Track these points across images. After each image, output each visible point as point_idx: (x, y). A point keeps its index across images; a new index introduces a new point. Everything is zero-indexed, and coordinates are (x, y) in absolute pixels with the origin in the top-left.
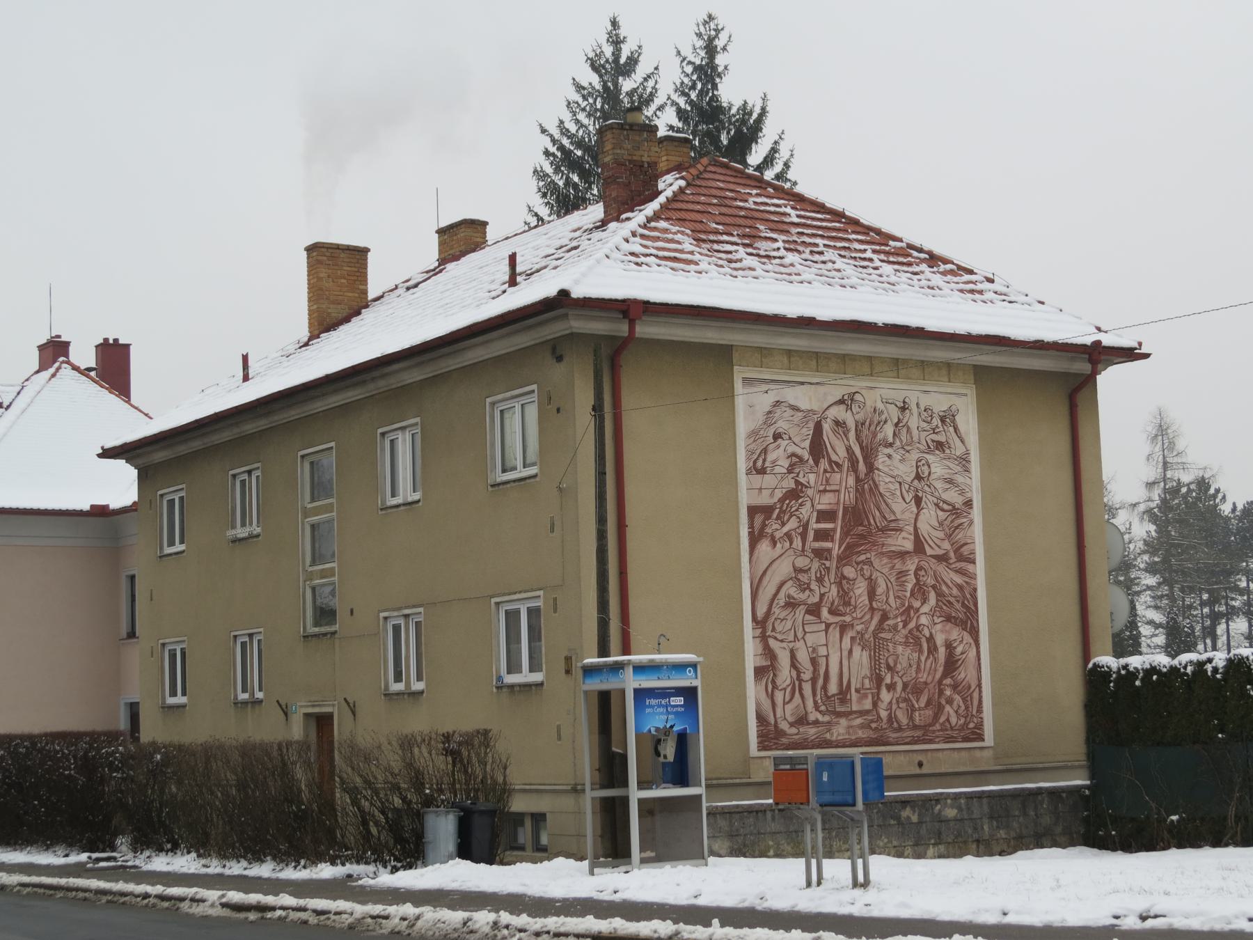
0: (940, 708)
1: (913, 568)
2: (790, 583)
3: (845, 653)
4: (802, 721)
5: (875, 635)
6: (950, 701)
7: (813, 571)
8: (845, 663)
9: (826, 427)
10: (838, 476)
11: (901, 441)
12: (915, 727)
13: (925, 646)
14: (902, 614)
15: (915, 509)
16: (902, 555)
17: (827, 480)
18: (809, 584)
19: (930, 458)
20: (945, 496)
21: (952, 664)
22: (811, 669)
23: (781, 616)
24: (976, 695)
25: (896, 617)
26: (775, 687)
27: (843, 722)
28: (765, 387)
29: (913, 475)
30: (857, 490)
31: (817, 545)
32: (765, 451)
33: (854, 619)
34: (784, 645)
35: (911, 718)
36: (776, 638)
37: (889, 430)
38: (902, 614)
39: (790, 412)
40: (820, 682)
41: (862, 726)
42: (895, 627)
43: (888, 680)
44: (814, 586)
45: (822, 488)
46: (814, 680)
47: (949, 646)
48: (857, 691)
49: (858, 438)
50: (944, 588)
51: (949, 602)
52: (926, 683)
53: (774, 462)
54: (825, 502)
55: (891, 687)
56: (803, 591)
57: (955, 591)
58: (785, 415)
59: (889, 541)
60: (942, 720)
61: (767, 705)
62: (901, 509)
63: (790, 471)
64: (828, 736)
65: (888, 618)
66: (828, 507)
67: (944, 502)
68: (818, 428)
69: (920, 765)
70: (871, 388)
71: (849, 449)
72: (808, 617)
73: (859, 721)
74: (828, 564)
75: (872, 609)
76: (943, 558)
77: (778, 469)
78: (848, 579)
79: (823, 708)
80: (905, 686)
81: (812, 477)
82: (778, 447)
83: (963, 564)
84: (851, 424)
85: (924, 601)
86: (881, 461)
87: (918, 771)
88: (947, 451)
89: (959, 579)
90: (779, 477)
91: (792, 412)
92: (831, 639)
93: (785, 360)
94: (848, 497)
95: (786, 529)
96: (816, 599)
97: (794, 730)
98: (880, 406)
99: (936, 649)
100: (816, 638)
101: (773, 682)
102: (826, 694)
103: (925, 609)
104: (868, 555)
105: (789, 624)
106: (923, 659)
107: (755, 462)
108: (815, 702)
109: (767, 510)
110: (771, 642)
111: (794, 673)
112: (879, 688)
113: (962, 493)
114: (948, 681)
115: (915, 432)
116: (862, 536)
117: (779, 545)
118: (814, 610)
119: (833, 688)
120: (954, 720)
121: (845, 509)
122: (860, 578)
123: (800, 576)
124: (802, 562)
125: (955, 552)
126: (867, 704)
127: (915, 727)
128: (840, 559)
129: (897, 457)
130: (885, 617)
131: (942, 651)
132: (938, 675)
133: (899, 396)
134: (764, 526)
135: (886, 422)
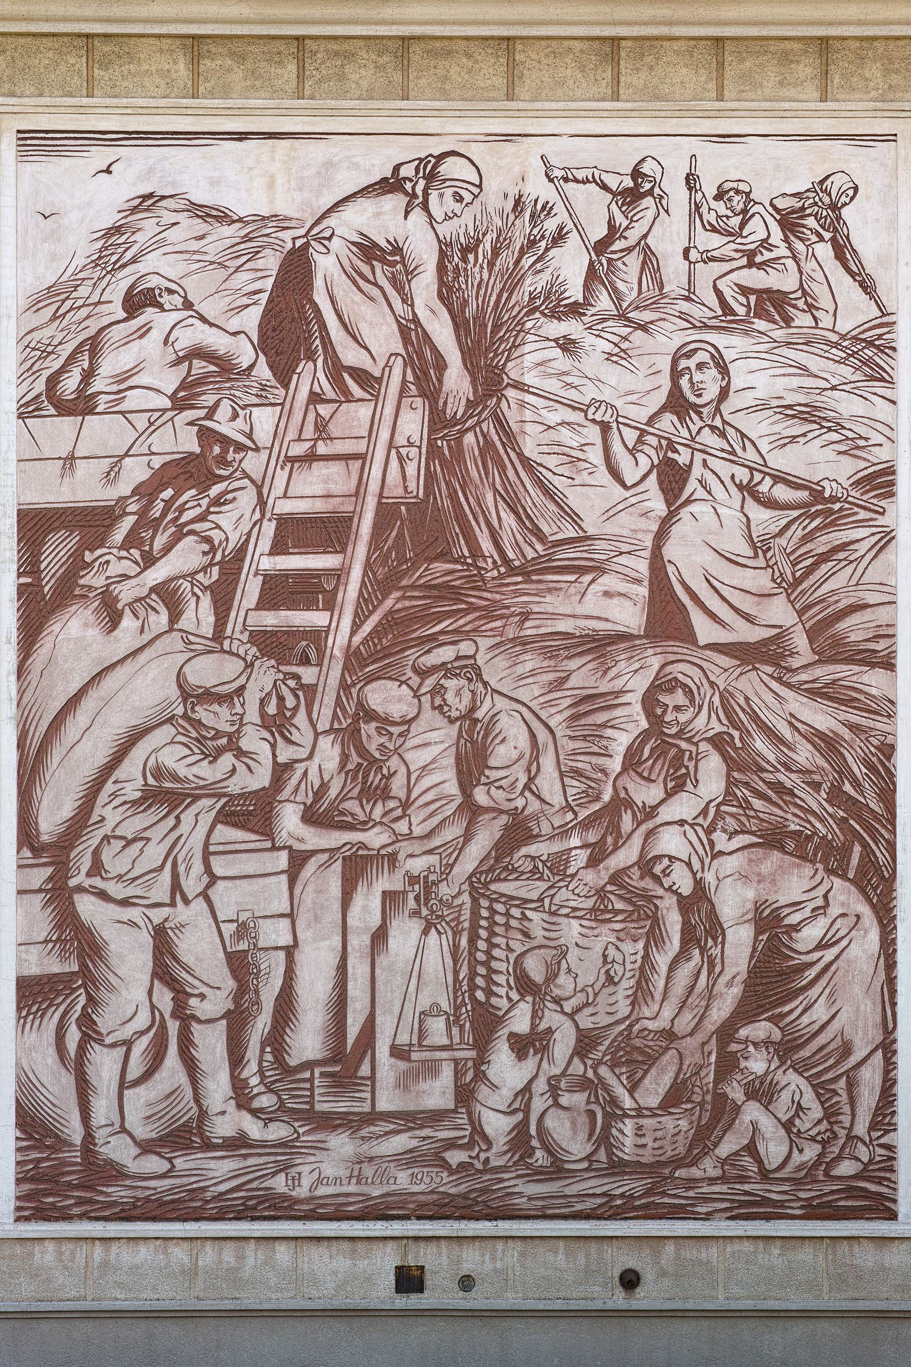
0: (723, 1112)
1: (641, 684)
2: (167, 731)
3: (359, 942)
4: (184, 1135)
5: (477, 885)
6: (762, 1092)
7: (252, 697)
8: (358, 969)
9: (325, 265)
10: (364, 412)
11: (616, 296)
12: (617, 1168)
13: (673, 921)
14: (587, 824)
15: (659, 506)
16: (601, 645)
17: (321, 427)
18: (233, 738)
19: (731, 345)
20: (779, 461)
21: (776, 977)
22: (230, 984)
23: (129, 829)
24: (870, 1077)
25: (564, 832)
26: (90, 1033)
27: (341, 1144)
28: (101, 156)
29: (660, 398)
30: (433, 451)
31: (270, 619)
32: (93, 346)
33: (398, 838)
34: (134, 914)
35: (604, 1139)
36: (103, 895)
37: (570, 266)
38: (587, 824)
39: (189, 226)
40: (262, 1023)
41: (409, 1159)
42: (558, 865)
43: (520, 1021)
44: (253, 740)
45: (298, 449)
46: (237, 1021)
47: (770, 923)
48: (398, 1052)
49: (446, 292)
50: (760, 744)
51: (778, 787)
52: (669, 1035)
53: (123, 377)
54: (310, 491)
55: (522, 1046)
56: (214, 756)
57: (804, 754)
58: (172, 235)
59: (552, 603)
60: (725, 1149)
61: (58, 1087)
62: (605, 504)
63: (182, 400)
64: (279, 1184)
65: (531, 838)
66: (319, 506)
67: (779, 478)
68: (297, 269)
69: (630, 1281)
70: (508, 137)
71: (411, 332)
72: (224, 833)
73: (401, 1142)
74: (308, 675)
75: (471, 810)
76: (766, 653)
77: (134, 400)
78: (384, 722)
79: (265, 1101)
80: (585, 1043)
81: (264, 421)
82: (144, 331)
83: (842, 671)
84: (422, 249)
85: (678, 785)
86: (533, 360)
87: (619, 1299)
88: (803, 320)
89: (821, 717)
90: (141, 422)
91: (200, 227)
92: (308, 897)
93: (182, 69)
94: (399, 476)
95: (157, 574)
96: (261, 779)
97: (154, 1164)
98: (540, 189)
99: (716, 929)
100: (252, 888)
101: (86, 1022)
102: (279, 1060)
103: (683, 807)
104: (466, 648)
105: (155, 853)
106: (662, 961)
107: (53, 381)
108: (239, 1087)
109: (92, 523)
110: (87, 907)
111: (165, 999)
112: (482, 1044)
113: (854, 447)
114: (761, 1029)
115: (674, 272)
116: (446, 591)
117: (128, 623)
118: (252, 814)
119: (308, 1041)
120: (774, 1149)
121: (386, 513)
122: (428, 714)
123: (202, 713)
124: (207, 672)
125: (812, 635)
126: (437, 1093)
127: (617, 1168)
128: (354, 659)
129: (596, 346)
130: (518, 831)
131: (740, 942)
132: (720, 1012)
133: (617, 160)
134: (77, 565)
135: (559, 237)
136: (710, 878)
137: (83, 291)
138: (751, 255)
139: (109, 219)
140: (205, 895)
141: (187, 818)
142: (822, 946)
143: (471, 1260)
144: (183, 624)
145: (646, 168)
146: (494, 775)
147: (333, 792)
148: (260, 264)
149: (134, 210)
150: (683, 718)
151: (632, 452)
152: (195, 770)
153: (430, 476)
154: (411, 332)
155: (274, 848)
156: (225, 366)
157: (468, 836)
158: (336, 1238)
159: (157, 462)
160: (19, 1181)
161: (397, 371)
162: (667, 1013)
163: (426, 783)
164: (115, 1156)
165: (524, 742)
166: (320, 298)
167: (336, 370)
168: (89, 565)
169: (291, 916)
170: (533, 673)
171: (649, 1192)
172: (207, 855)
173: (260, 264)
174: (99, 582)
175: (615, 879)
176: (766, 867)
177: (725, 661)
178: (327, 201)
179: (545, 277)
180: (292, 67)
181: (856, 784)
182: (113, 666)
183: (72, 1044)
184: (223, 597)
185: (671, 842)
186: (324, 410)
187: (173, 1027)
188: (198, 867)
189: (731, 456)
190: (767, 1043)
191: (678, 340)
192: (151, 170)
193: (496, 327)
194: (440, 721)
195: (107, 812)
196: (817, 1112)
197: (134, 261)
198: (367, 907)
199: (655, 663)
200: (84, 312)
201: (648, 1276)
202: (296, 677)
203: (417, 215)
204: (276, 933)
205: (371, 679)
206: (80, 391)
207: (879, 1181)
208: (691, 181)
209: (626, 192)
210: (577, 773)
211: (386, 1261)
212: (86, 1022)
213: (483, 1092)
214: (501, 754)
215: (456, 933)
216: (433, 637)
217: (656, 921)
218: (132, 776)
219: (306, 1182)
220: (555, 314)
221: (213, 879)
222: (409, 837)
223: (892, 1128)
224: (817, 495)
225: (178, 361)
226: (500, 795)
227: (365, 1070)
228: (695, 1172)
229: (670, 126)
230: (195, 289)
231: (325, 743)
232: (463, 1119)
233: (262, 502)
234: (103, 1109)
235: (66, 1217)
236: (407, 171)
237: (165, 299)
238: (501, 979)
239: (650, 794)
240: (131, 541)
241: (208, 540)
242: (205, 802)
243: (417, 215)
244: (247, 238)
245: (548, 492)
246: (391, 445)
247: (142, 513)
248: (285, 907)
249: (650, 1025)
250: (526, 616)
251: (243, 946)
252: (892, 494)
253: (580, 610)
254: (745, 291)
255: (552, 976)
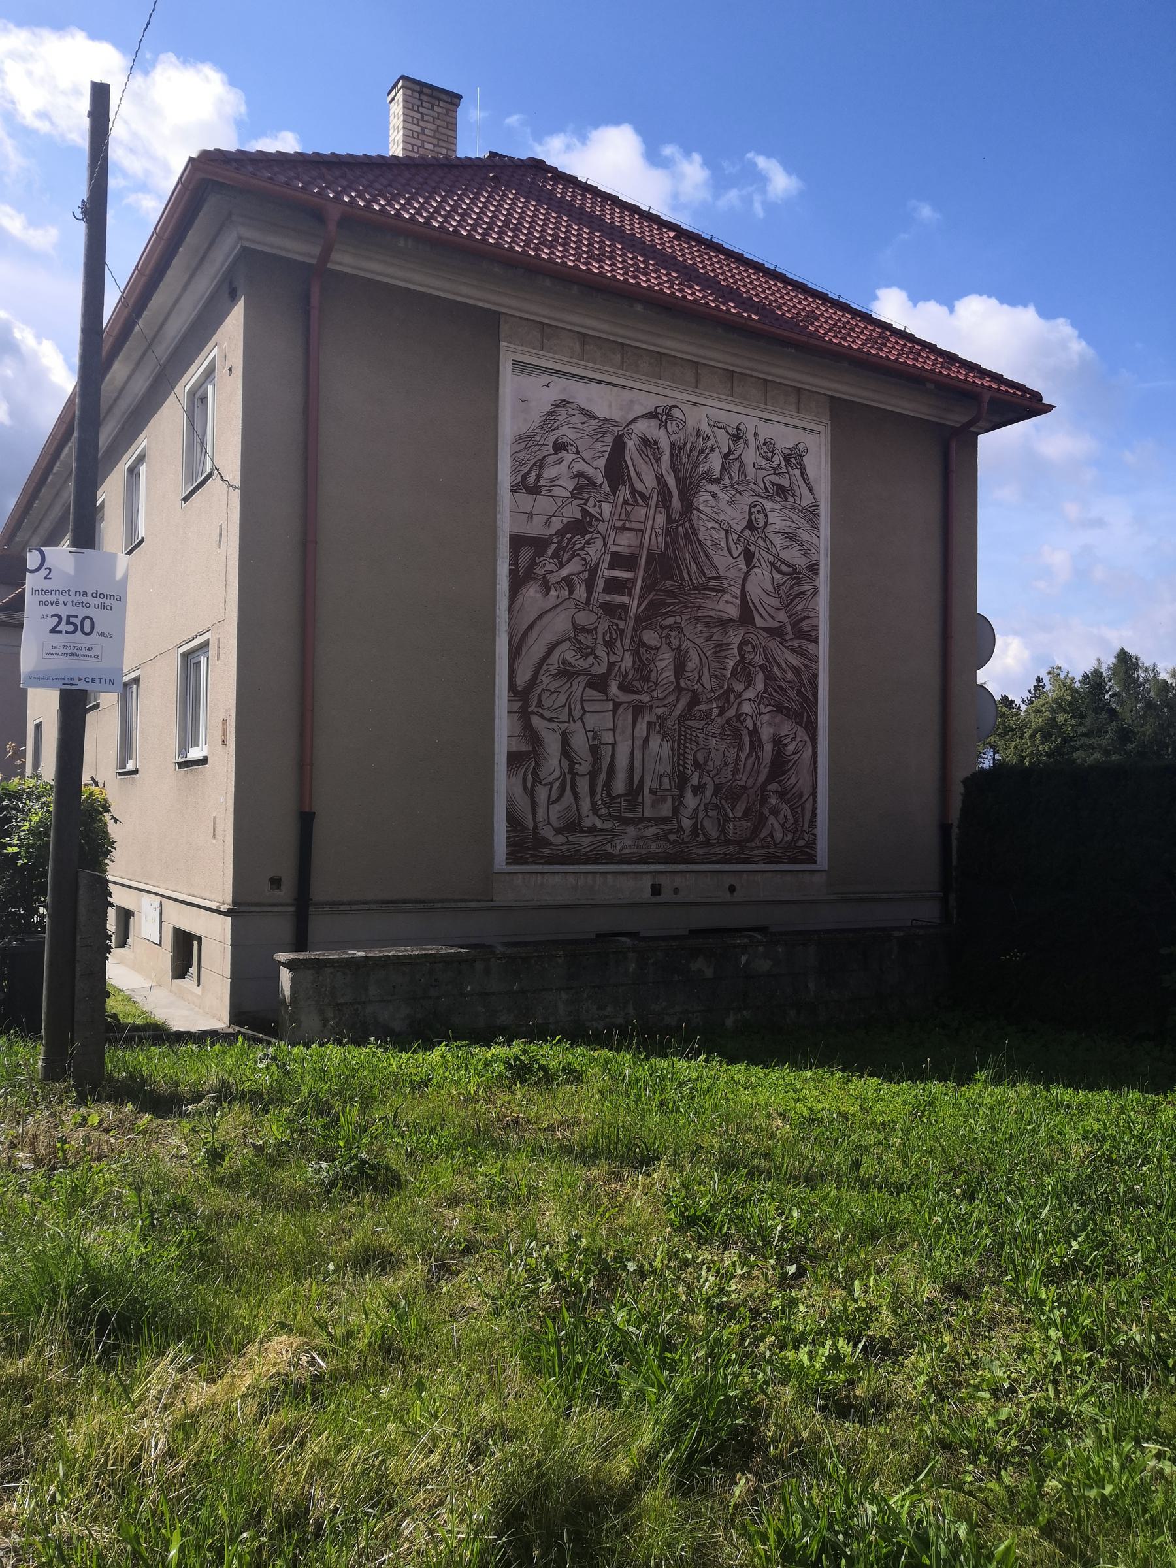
0: (762, 820)
1: (737, 641)
2: (567, 644)
3: (639, 743)
4: (572, 826)
5: (681, 721)
6: (775, 812)
7: (600, 631)
8: (638, 755)
9: (630, 445)
10: (643, 511)
11: (731, 478)
12: (728, 842)
13: (747, 740)
14: (718, 698)
15: (744, 567)
16: (724, 623)
17: (627, 515)
18: (593, 649)
19: (769, 505)
20: (784, 555)
21: (780, 765)
22: (590, 759)
23: (552, 687)
24: (809, 806)
25: (711, 702)
26: (537, 780)
27: (631, 831)
28: (546, 378)
29: (744, 523)
30: (668, 533)
31: (608, 598)
32: (541, 464)
33: (653, 699)
34: (553, 725)
35: (723, 831)
36: (541, 716)
37: (716, 461)
38: (718, 698)
39: (578, 418)
40: (602, 777)
41: (655, 838)
42: (708, 714)
43: (695, 781)
44: (601, 651)
45: (619, 524)
46: (593, 775)
47: (777, 742)
48: (652, 792)
49: (673, 465)
50: (776, 670)
51: (781, 687)
52: (745, 787)
53: (552, 480)
54: (623, 543)
55: (698, 790)
56: (586, 656)
57: (790, 675)
58: (572, 420)
59: (708, 603)
60: (762, 835)
61: (523, 802)
62: (726, 563)
63: (575, 495)
64: (608, 848)
65: (699, 703)
66: (626, 550)
67: (783, 562)
68: (619, 445)
69: (732, 889)
70: (696, 404)
71: (660, 479)
72: (590, 692)
73: (653, 831)
74: (621, 624)
75: (679, 689)
76: (776, 632)
77: (557, 491)
78: (649, 647)
79: (603, 812)
80: (717, 789)
81: (606, 508)
82: (561, 461)
83: (803, 642)
84: (665, 444)
85: (749, 684)
86: (703, 498)
87: (728, 897)
88: (791, 499)
89: (795, 661)
90: (559, 501)
91: (584, 419)
92: (620, 723)
93: (577, 347)
94: (654, 540)
95: (565, 572)
96: (603, 669)
97: (561, 839)
98: (705, 428)
99: (760, 745)
100: (599, 719)
101: (535, 773)
102: (609, 794)
103: (750, 694)
104: (678, 619)
105: (562, 699)
106: (743, 757)
107: (525, 477)
108: (594, 804)
109: (539, 544)
110: (536, 721)
111: (566, 765)
112: (682, 790)
113: (806, 553)
114: (774, 786)
115: (750, 470)
116: (671, 594)
117: (553, 593)
118: (599, 683)
119: (619, 786)
120: (778, 835)
121: (650, 556)
122: (664, 646)
123: (581, 637)
124: (584, 619)
125: (793, 626)
126: (665, 810)
127: (728, 842)
128: (638, 619)
129: (724, 497)
130: (695, 700)
131: (768, 748)
132: (761, 779)
133: (733, 420)
134: (533, 564)
135: (712, 450)
136: (759, 724)
137: (537, 438)
138: (775, 469)
139: (548, 408)
140: (581, 719)
141: (575, 684)
142: (794, 753)
143: (678, 881)
144: (573, 596)
145: (741, 427)
146: (688, 674)
147: (630, 677)
148: (605, 439)
149: (558, 406)
150: (751, 656)
151: (735, 543)
152: (578, 662)
153: (666, 543)
154: (660, 479)
155: (608, 700)
156: (591, 481)
157: (678, 700)
158: (614, 905)
159: (565, 521)
160: (507, 846)
161: (655, 495)
162: (744, 779)
163: (664, 676)
164: (546, 835)
165: (697, 661)
166: (628, 459)
167: (633, 491)
168: (538, 564)
169: (614, 730)
170: (701, 633)
171: (738, 853)
172: (582, 701)
173: (605, 439)
174: (542, 572)
175: (728, 721)
176: (777, 720)
177: (765, 635)
178: (631, 417)
179: (707, 465)
180: (619, 356)
181: (805, 689)
182: (546, 612)
183: (529, 784)
184: (590, 585)
185: (747, 708)
186: (629, 508)
187: (569, 777)
188: (579, 706)
189: (768, 551)
190: (776, 792)
191: (752, 499)
192: (565, 389)
193: (690, 483)
194: (668, 650)
195: (543, 678)
196: (792, 821)
197: (557, 428)
198: (642, 728)
199: (742, 632)
200: (537, 448)
201: (738, 887)
202: (617, 625)
203: (663, 430)
204: (608, 738)
205: (645, 628)
206: (535, 484)
207: (811, 848)
208: (756, 435)
209: (734, 436)
210: (716, 676)
211: (647, 882)
212: (535, 773)
213: (682, 809)
214: (691, 666)
215: (673, 741)
216: (666, 613)
217: (741, 740)
218: (554, 663)
219: (618, 847)
220: (710, 482)
221: (585, 712)
222: (657, 699)
223: (815, 827)
224: (795, 570)
225: (574, 477)
226: (689, 683)
227: (640, 799)
228: (753, 845)
229: (749, 411)
230: (582, 445)
231: (627, 655)
232: (675, 821)
233: (605, 545)
234: (541, 813)
235: (526, 863)
236: (660, 410)
237: (569, 448)
238: (688, 762)
239: (739, 687)
240: (555, 555)
241: (584, 559)
242: (582, 677)
243: (663, 430)
244: (601, 427)
245: (707, 556)
246: (653, 528)
247: (559, 543)
248: (610, 726)
249: (739, 783)
250: (699, 608)
251: (595, 743)
252: (817, 574)
253: (718, 607)
254: (773, 484)
255: (706, 761)
